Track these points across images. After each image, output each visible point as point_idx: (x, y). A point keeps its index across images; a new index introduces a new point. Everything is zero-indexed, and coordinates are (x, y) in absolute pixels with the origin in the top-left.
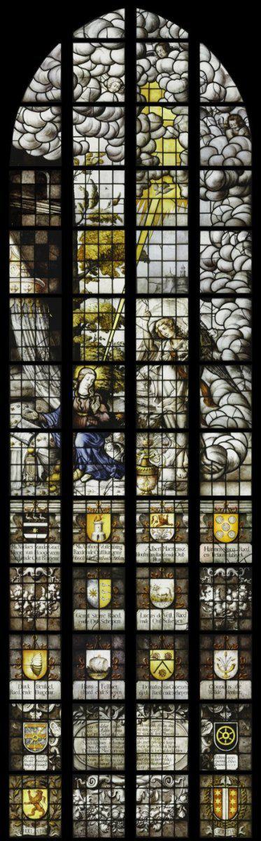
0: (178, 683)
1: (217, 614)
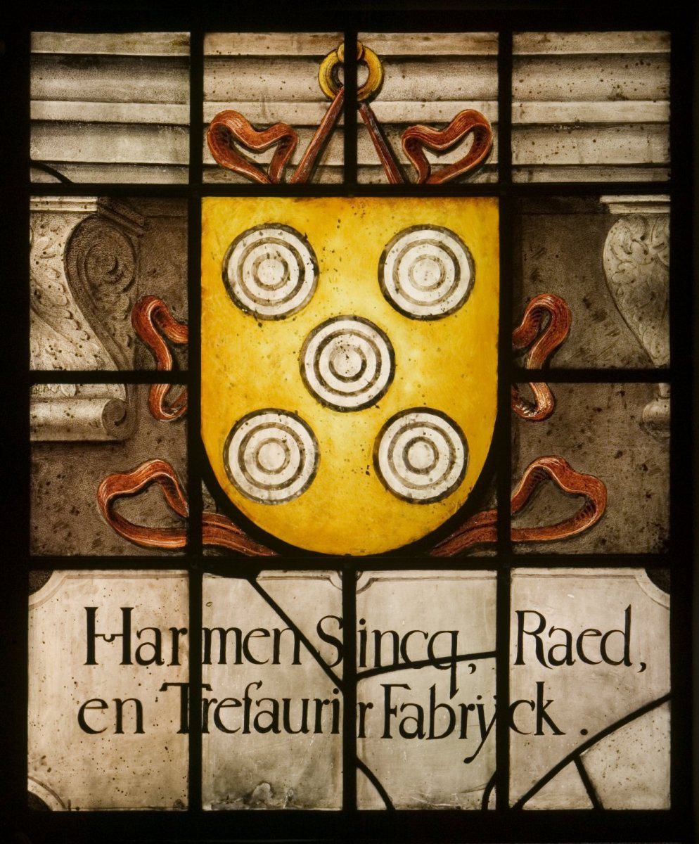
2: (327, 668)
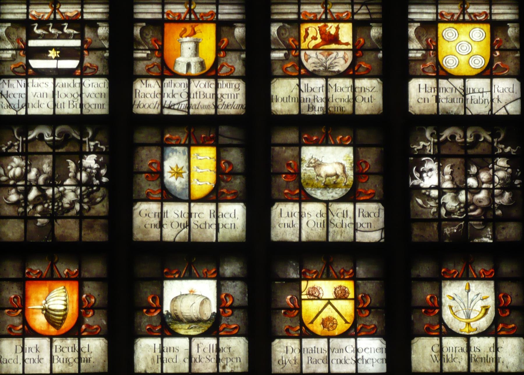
0: (364, 342)
1: (448, 213)
2: (461, 93)
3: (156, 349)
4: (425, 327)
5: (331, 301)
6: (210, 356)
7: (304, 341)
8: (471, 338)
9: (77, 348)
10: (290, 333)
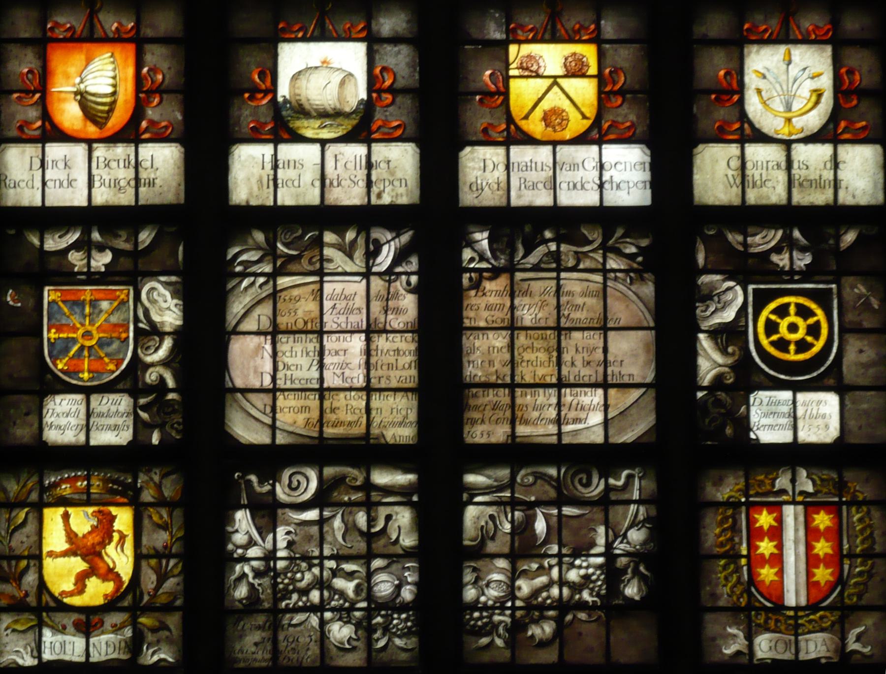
0: (613, 152)
3: (265, 164)
4: (717, 125)
5: (559, 80)
6: (356, 176)
7: (514, 150)
8: (794, 146)
9: (133, 162)
10: (490, 136)
